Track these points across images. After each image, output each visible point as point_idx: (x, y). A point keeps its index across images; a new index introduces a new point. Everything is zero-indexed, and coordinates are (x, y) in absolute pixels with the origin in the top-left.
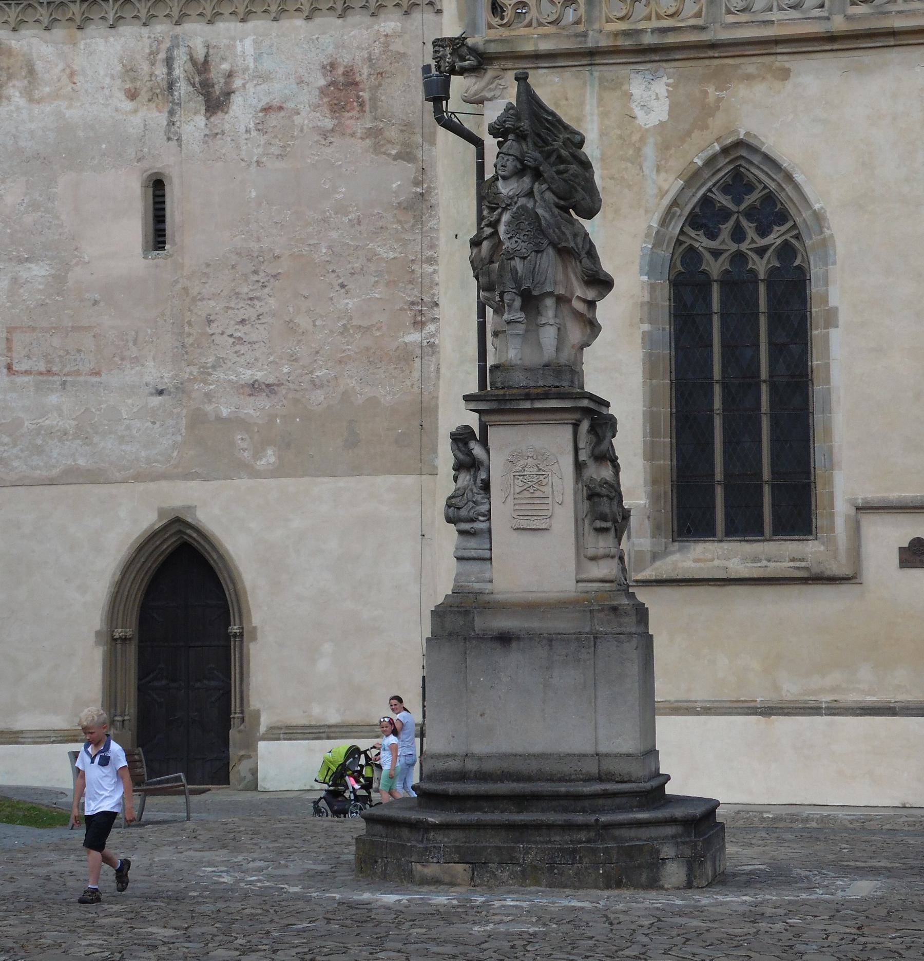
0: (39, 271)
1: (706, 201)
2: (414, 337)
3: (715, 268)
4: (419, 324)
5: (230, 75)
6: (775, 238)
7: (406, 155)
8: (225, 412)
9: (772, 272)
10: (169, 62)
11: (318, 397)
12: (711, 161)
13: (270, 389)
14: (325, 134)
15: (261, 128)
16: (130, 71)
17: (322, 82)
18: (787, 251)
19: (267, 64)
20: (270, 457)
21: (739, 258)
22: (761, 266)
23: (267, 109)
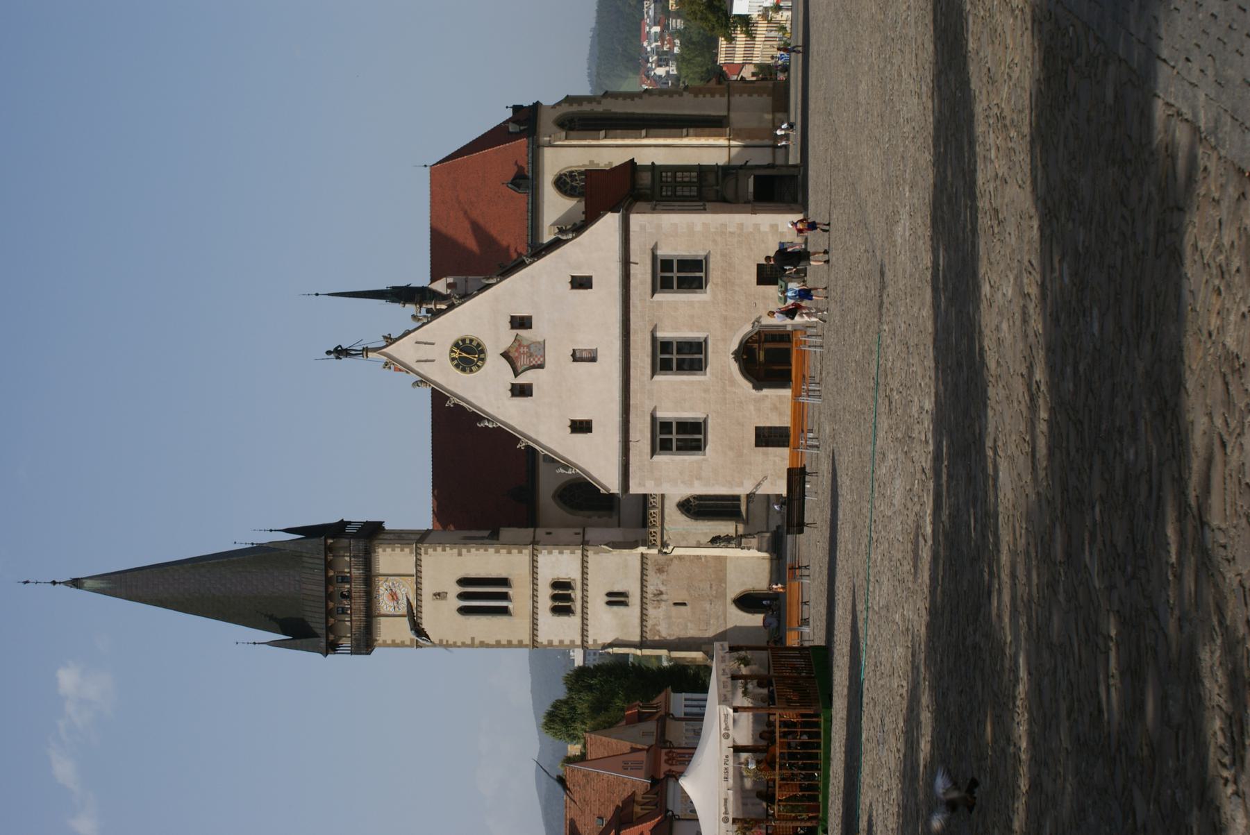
0: (689, 624)
1: (686, 511)
2: (703, 559)
3: (697, 509)
4: (701, 558)
5: (657, 590)
6: (692, 500)
7: (672, 560)
8: (715, 592)
9: (698, 500)
10: (654, 601)
11: (713, 576)
12: (680, 510)
13: (711, 585)
14: (668, 574)
15: (666, 585)
16: (655, 608)
17: (658, 575)
18: (694, 498)
19: (655, 584)
20: (723, 585)
21: (695, 505)
22: (697, 502)
23: (663, 584)
